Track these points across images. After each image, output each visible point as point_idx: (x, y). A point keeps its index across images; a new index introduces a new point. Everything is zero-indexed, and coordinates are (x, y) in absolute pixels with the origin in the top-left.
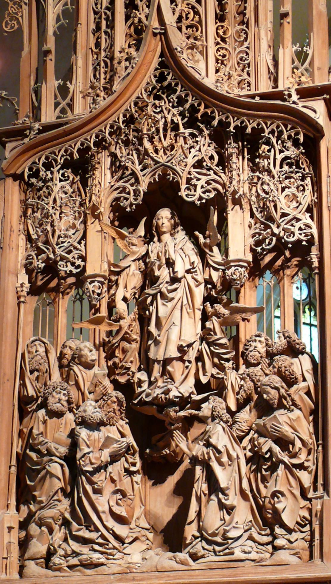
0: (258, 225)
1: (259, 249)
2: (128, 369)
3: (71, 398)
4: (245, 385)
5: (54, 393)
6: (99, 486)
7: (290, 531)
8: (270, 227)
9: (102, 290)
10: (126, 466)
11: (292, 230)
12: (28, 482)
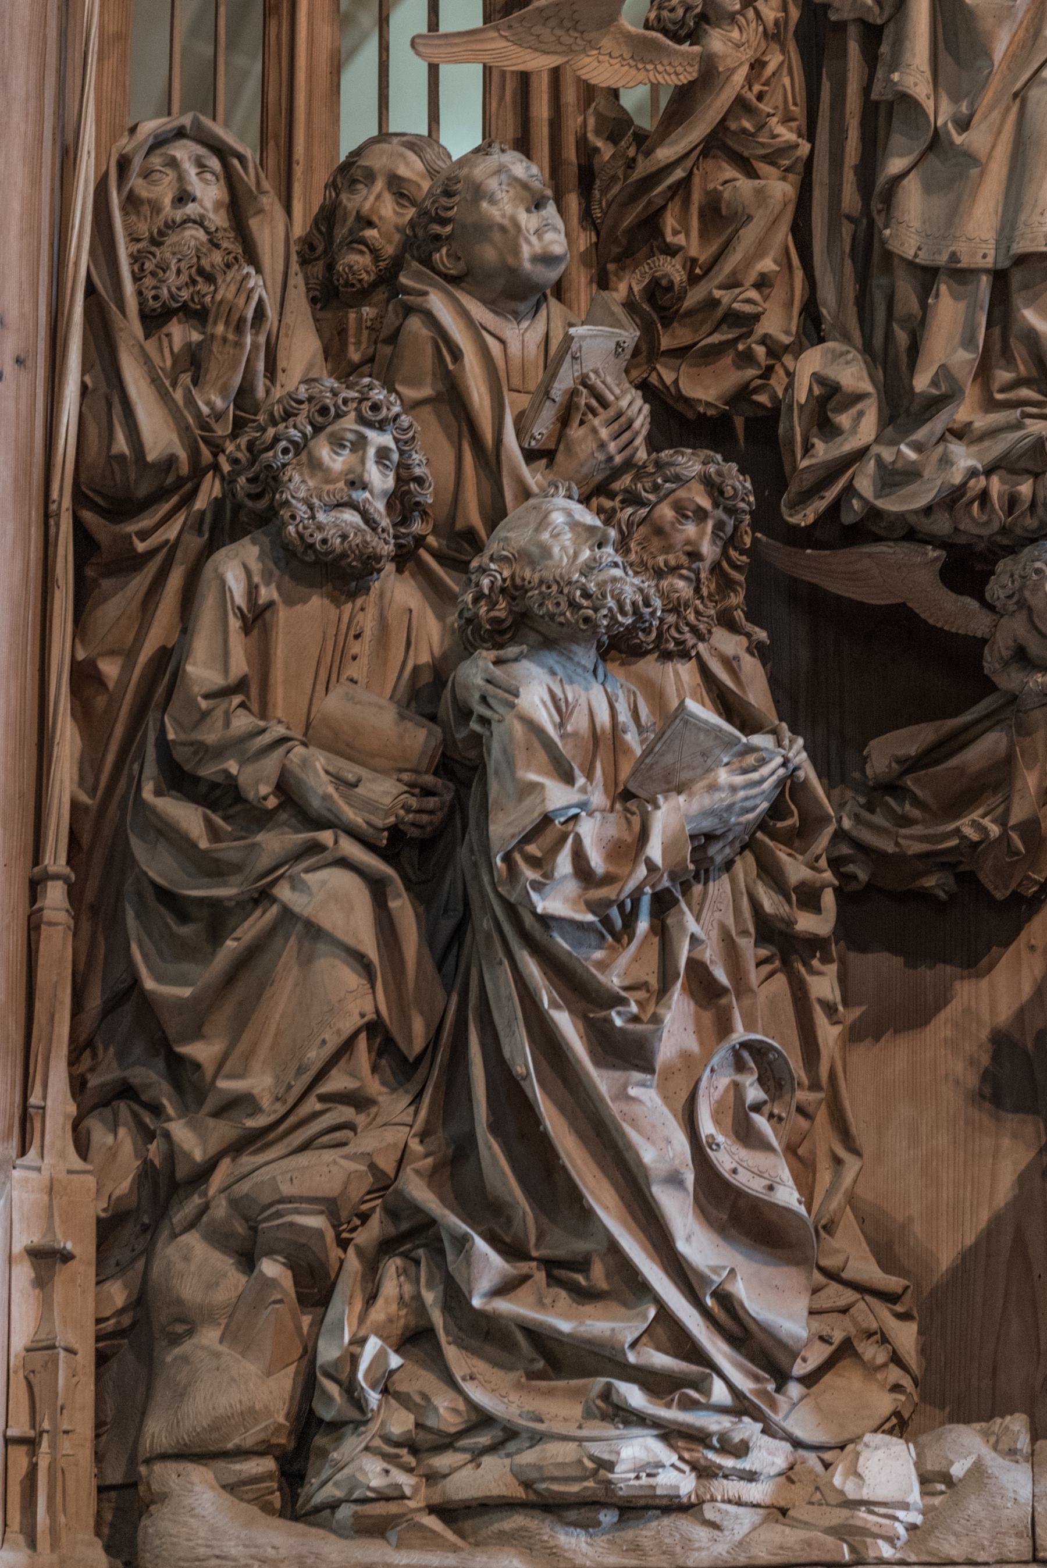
2: (748, 321)
3: (420, 481)
5: (324, 452)
6: (635, 1019)
10: (770, 902)
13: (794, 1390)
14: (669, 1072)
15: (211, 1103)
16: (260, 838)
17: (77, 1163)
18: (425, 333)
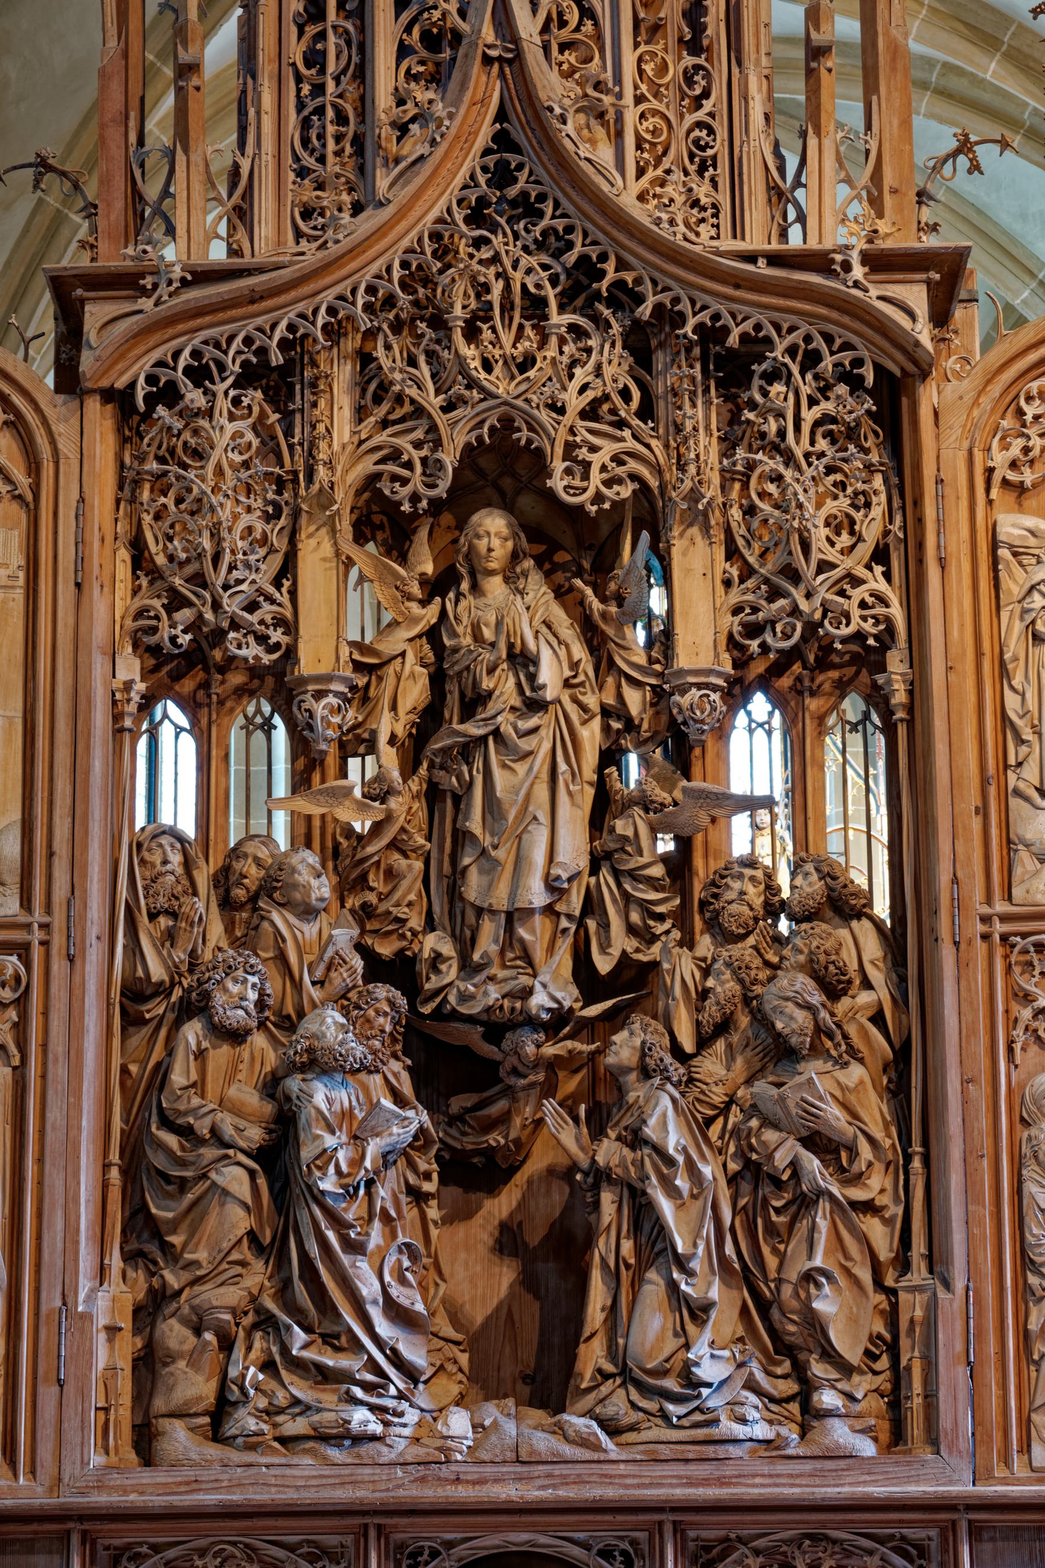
0: (750, 583)
1: (754, 645)
2: (404, 921)
4: (719, 989)
5: (230, 985)
6: (359, 1234)
7: (847, 1370)
8: (785, 595)
9: (344, 716)
10: (412, 1179)
11: (846, 607)
12: (154, 1210)
13: (421, 1386)
14: (372, 1254)
15: (181, 1263)
16: (202, 1151)
17: (124, 1288)
18: (271, 929)
